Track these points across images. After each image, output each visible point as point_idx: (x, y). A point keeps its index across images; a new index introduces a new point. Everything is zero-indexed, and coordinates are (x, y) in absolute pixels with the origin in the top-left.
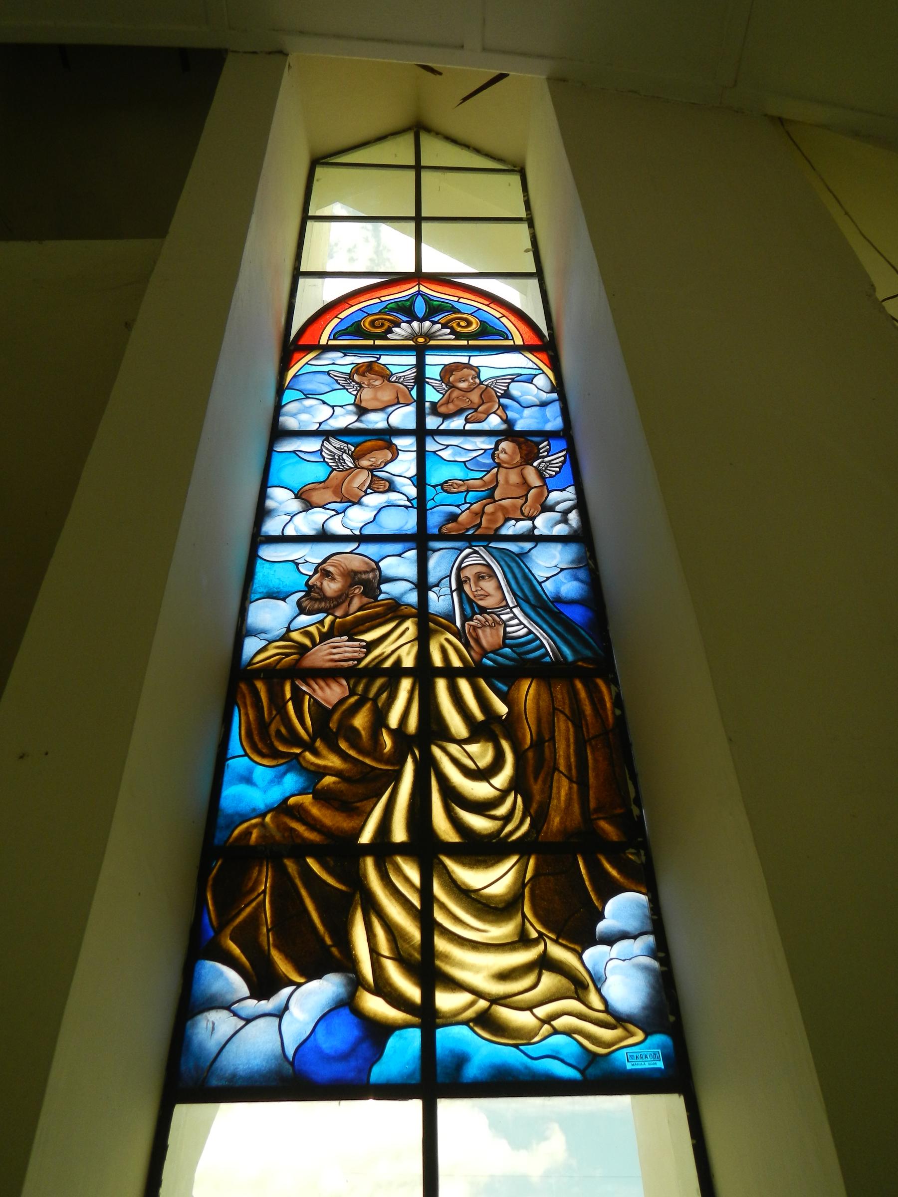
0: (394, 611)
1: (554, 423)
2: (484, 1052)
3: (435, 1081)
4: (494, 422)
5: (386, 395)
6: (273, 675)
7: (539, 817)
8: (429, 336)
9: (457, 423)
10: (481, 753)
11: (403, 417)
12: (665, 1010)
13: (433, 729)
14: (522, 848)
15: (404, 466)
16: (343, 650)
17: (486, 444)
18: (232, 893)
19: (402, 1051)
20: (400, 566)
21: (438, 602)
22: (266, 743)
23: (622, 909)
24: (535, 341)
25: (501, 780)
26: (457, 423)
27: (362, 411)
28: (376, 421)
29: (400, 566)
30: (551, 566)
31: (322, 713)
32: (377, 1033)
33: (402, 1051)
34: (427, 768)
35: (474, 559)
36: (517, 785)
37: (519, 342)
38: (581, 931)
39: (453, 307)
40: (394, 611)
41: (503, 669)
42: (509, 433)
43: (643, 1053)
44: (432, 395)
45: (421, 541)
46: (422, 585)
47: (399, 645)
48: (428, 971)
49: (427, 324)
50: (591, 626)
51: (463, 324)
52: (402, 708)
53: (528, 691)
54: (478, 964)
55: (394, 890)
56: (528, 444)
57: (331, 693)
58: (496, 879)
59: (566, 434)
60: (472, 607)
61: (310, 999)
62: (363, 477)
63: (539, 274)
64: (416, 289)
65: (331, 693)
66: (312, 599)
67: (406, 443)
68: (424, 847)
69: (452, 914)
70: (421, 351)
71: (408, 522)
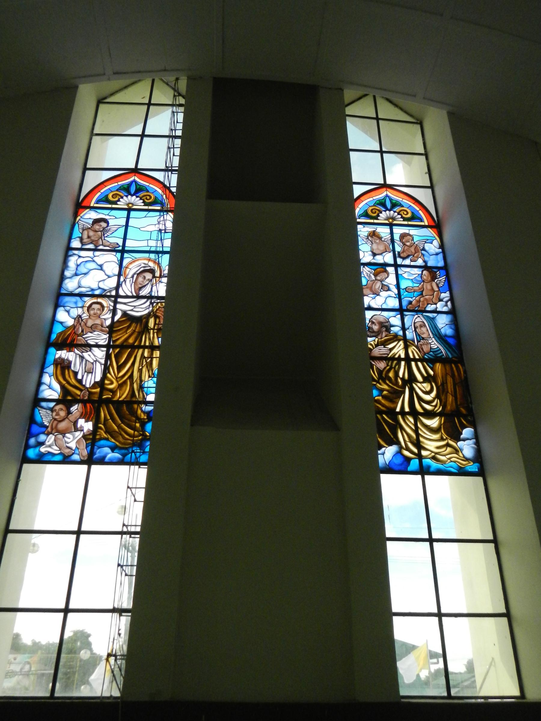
0: (396, 338)
1: (441, 264)
2: (434, 465)
3: (423, 471)
4: (420, 262)
5: (382, 248)
7: (444, 406)
8: (394, 219)
9: (407, 262)
10: (426, 386)
11: (388, 258)
12: (478, 457)
13: (412, 379)
14: (440, 415)
15: (391, 280)
17: (417, 271)
19: (414, 464)
20: (395, 320)
21: (410, 335)
23: (467, 432)
24: (432, 224)
25: (434, 394)
26: (407, 262)
27: (374, 255)
28: (379, 259)
29: (395, 320)
30: (443, 322)
31: (380, 372)
32: (408, 460)
33: (414, 464)
34: (412, 390)
35: (419, 319)
36: (438, 396)
37: (427, 224)
38: (457, 437)
39: (401, 204)
40: (396, 338)
41: (431, 360)
42: (425, 267)
43: (473, 467)
44: (398, 249)
45: (401, 311)
46: (404, 329)
47: (399, 350)
48: (420, 446)
49: (392, 212)
51: (405, 213)
53: (438, 366)
54: (431, 444)
56: (431, 270)
57: (382, 365)
58: (434, 423)
59: (445, 268)
60: (420, 338)
62: (378, 285)
63: (432, 187)
64: (385, 194)
65: (382, 365)
67: (391, 270)
68: (414, 413)
69: (423, 431)
70: (391, 226)
71: (394, 303)
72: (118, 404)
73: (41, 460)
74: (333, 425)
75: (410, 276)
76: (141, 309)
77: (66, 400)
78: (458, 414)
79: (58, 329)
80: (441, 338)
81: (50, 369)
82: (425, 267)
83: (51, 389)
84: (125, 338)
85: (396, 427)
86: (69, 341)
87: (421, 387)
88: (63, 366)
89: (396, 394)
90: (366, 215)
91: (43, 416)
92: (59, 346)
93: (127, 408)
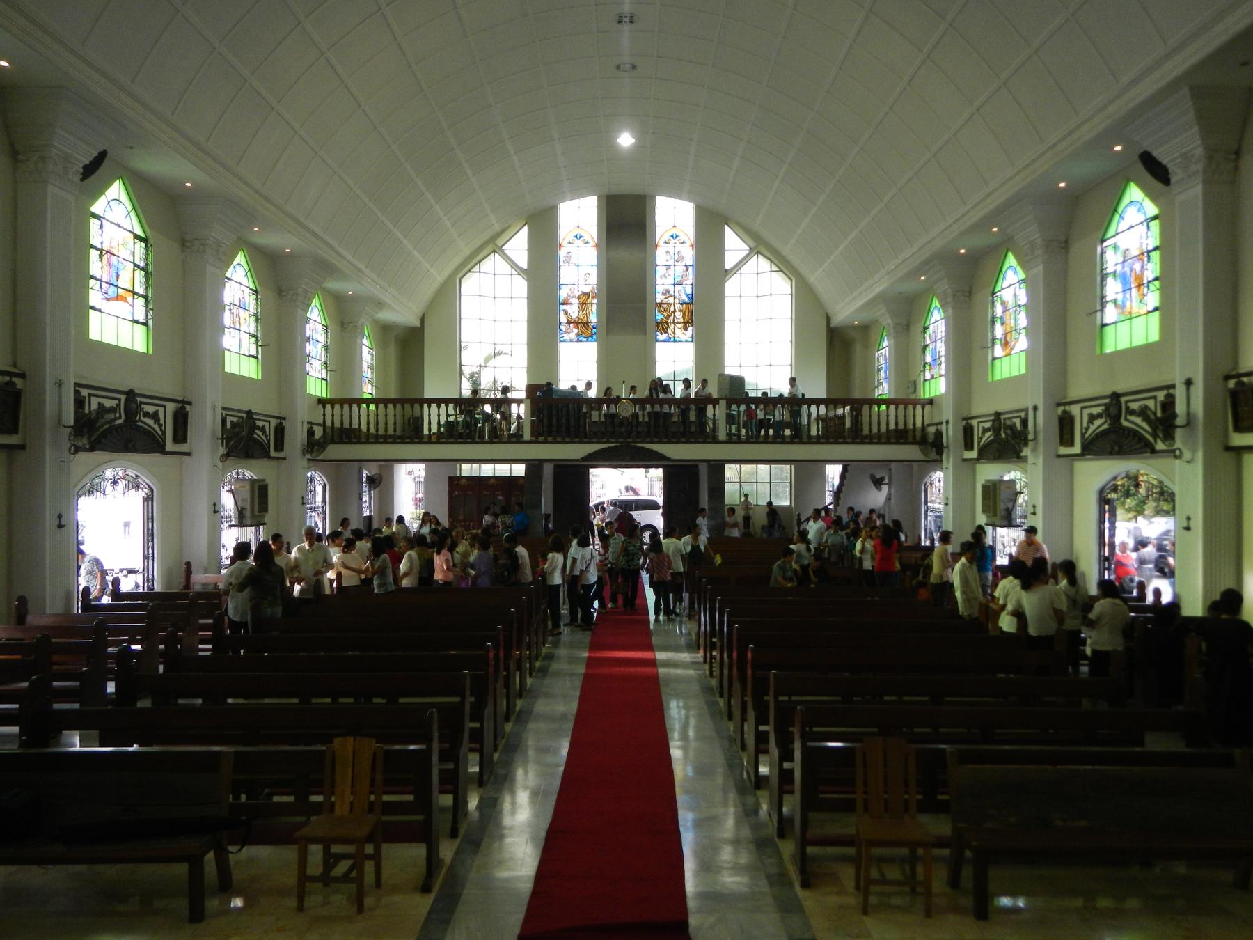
11: (671, 262)
38: (686, 329)
47: (671, 300)
54: (677, 331)
55: (672, 326)
56: (687, 267)
61: (665, 335)
75: (680, 269)
76: (587, 289)
77: (569, 323)
83: (563, 319)
84: (584, 301)
86: (565, 303)
87: (677, 314)
88: (566, 312)
89: (669, 316)
91: (563, 328)
93: (586, 324)
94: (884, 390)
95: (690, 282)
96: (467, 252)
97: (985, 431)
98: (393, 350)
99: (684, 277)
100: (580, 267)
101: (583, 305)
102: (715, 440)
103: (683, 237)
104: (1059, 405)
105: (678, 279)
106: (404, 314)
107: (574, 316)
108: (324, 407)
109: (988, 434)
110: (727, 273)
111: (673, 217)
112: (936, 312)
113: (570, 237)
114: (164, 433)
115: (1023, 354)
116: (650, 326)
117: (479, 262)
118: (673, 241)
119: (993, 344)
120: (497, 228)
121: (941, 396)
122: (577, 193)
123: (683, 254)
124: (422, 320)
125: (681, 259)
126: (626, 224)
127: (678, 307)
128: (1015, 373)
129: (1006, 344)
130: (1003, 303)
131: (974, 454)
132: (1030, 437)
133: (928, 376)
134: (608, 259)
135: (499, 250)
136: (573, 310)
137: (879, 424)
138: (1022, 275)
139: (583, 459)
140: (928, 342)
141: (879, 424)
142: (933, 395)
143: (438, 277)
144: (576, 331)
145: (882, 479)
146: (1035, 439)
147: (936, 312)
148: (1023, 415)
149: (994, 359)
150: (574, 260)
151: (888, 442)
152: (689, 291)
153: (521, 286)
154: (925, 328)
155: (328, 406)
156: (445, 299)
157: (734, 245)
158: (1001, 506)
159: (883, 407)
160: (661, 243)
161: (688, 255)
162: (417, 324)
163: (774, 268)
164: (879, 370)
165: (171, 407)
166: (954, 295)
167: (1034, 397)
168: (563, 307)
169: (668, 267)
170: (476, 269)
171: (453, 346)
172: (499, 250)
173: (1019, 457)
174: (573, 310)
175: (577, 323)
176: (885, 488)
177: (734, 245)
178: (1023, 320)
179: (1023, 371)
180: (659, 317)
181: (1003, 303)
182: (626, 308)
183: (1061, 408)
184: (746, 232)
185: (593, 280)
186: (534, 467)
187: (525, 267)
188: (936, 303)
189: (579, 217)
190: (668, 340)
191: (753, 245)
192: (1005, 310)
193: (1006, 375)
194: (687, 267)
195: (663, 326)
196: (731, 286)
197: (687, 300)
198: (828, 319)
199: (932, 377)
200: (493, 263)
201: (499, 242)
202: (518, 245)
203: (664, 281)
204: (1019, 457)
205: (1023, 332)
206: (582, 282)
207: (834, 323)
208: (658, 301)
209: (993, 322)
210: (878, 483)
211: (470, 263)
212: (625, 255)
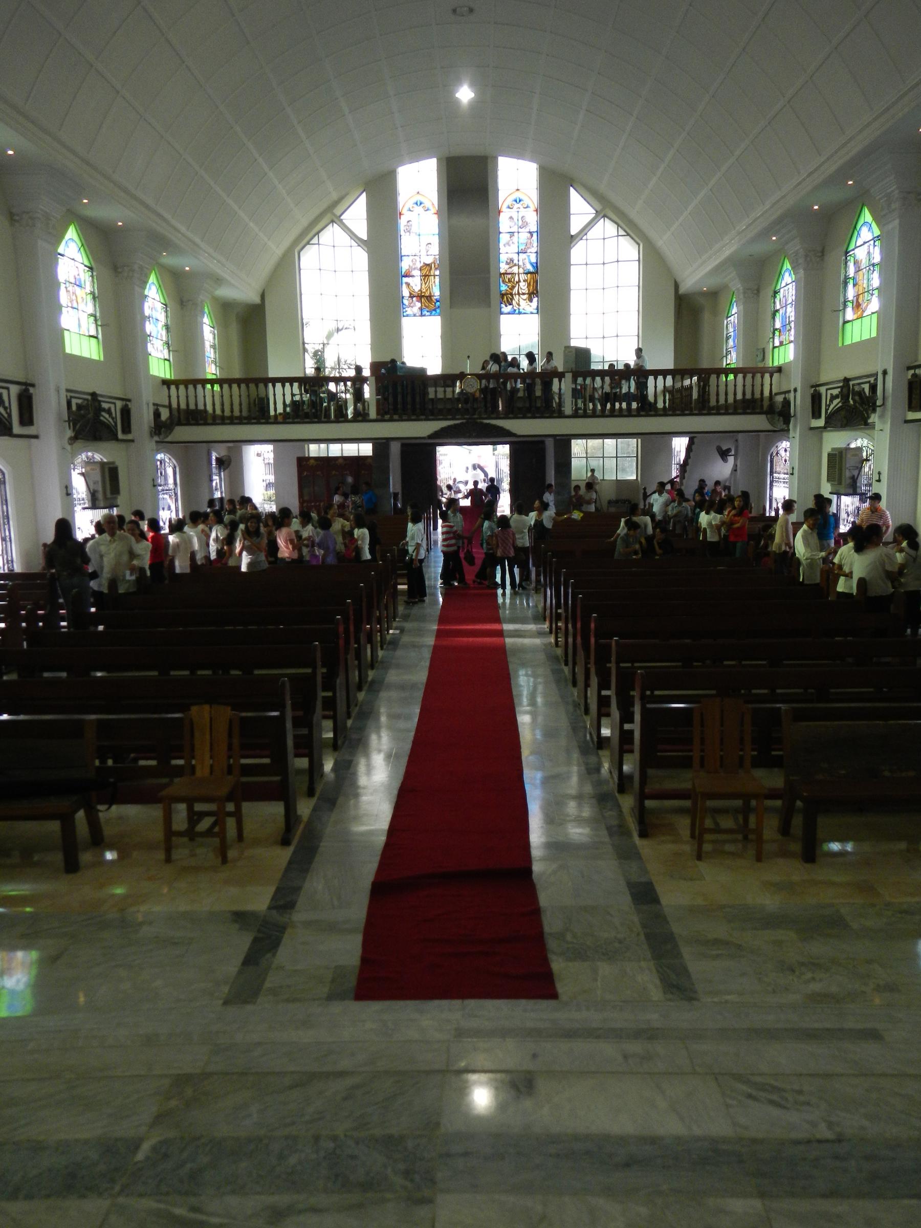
0: (515, 265)
3: (520, 313)
6: (504, 274)
11: (515, 229)
13: (519, 281)
16: (509, 271)
18: (503, 298)
21: (521, 263)
22: (504, 282)
38: (531, 300)
42: (530, 232)
47: (515, 270)
48: (519, 305)
50: (535, 266)
52: (517, 279)
54: (522, 303)
56: (531, 233)
58: (525, 297)
61: (509, 308)
65: (509, 276)
66: (507, 263)
68: (519, 294)
72: (427, 297)
73: (407, 316)
74: (489, 306)
75: (524, 236)
76: (429, 260)
78: (533, 293)
79: (404, 271)
80: (531, 264)
81: (404, 285)
82: (530, 232)
83: (406, 292)
85: (512, 299)
87: (522, 284)
88: (408, 284)
89: (513, 287)
90: (509, 207)
91: (406, 302)
92: (406, 276)
93: (429, 298)
94: (732, 359)
95: (534, 249)
96: (305, 222)
97: (833, 398)
98: (234, 330)
99: (528, 245)
100: (421, 236)
101: (425, 277)
102: (561, 415)
103: (526, 201)
104: (909, 368)
105: (522, 247)
106: (243, 291)
107: (417, 289)
108: (169, 388)
109: (835, 402)
110: (572, 239)
111: (517, 179)
112: (787, 274)
113: (410, 204)
114: (10, 415)
115: (875, 317)
116: (495, 297)
117: (318, 233)
118: (517, 206)
119: (845, 306)
120: (335, 196)
121: (790, 363)
122: (416, 155)
123: (527, 219)
124: (263, 296)
125: (525, 224)
126: (468, 189)
127: (522, 277)
128: (866, 337)
129: (857, 306)
130: (856, 263)
131: (821, 422)
132: (879, 403)
133: (777, 343)
134: (450, 227)
135: (337, 220)
136: (416, 283)
137: (726, 394)
138: (877, 232)
139: (430, 437)
140: (778, 307)
141: (726, 394)
142: (781, 362)
143: (277, 250)
144: (419, 305)
145: (729, 450)
146: (883, 404)
147: (787, 274)
148: (872, 380)
149: (845, 322)
150: (414, 229)
151: (735, 413)
152: (534, 260)
153: (362, 258)
154: (776, 293)
155: (173, 387)
156: (285, 272)
157: (580, 208)
158: (847, 474)
159: (731, 377)
160: (504, 209)
161: (532, 220)
162: (257, 300)
163: (622, 232)
164: (728, 338)
165: (15, 390)
166: (806, 256)
167: (884, 361)
168: (405, 280)
169: (512, 234)
170: (315, 241)
171: (295, 324)
172: (337, 220)
173: (866, 424)
174: (416, 283)
175: (420, 297)
176: (731, 460)
177: (580, 208)
178: (876, 282)
179: (874, 334)
180: (504, 288)
181: (856, 263)
182: (470, 279)
183: (912, 372)
184: (593, 194)
185: (435, 250)
186: (381, 445)
187: (364, 236)
188: (787, 265)
189: (419, 182)
190: (513, 312)
191: (599, 208)
192: (858, 270)
193: (856, 339)
194: (531, 233)
195: (507, 298)
196: (577, 253)
197: (532, 269)
198: (677, 286)
199: (781, 343)
200: (332, 234)
201: (337, 211)
202: (357, 214)
203: (507, 249)
204: (866, 424)
205: (876, 292)
206: (423, 253)
207: (682, 290)
208: (502, 271)
209: (846, 283)
210: (724, 454)
211: (308, 234)
212: (467, 222)
